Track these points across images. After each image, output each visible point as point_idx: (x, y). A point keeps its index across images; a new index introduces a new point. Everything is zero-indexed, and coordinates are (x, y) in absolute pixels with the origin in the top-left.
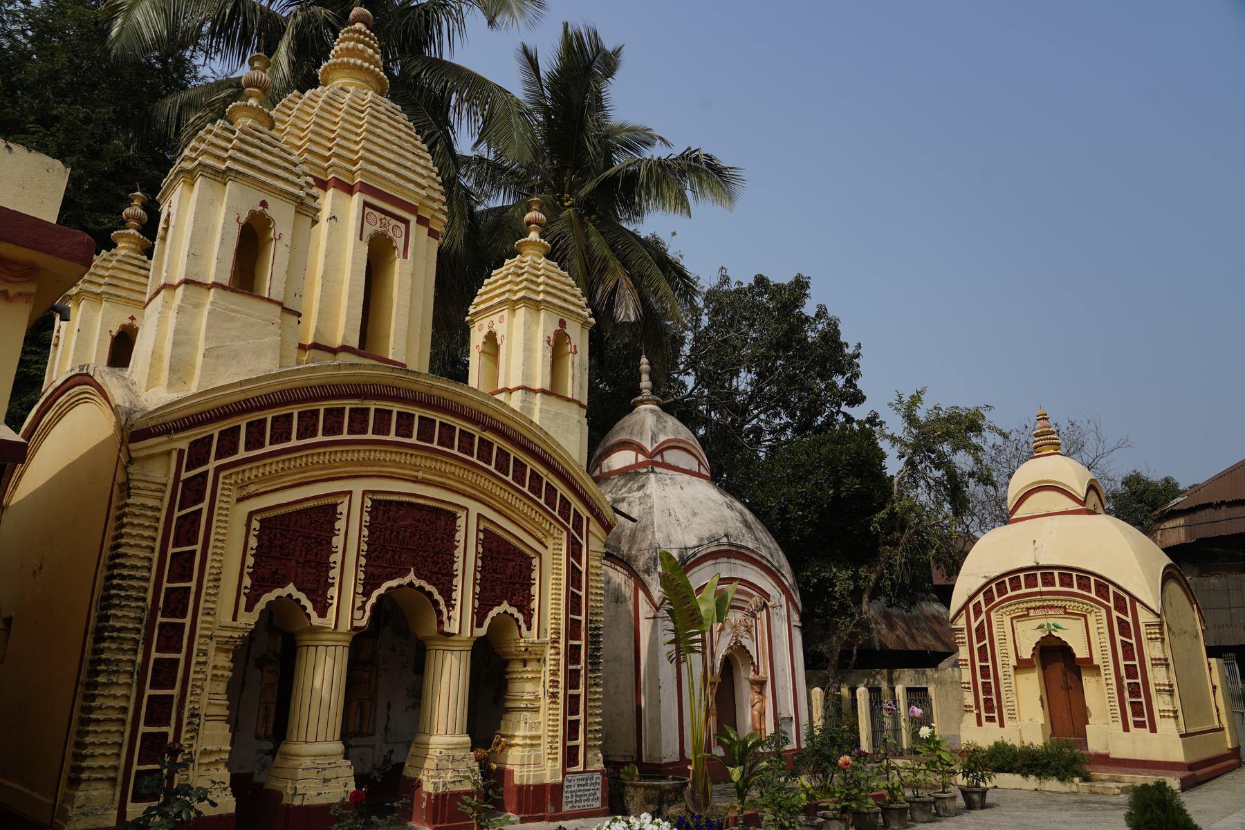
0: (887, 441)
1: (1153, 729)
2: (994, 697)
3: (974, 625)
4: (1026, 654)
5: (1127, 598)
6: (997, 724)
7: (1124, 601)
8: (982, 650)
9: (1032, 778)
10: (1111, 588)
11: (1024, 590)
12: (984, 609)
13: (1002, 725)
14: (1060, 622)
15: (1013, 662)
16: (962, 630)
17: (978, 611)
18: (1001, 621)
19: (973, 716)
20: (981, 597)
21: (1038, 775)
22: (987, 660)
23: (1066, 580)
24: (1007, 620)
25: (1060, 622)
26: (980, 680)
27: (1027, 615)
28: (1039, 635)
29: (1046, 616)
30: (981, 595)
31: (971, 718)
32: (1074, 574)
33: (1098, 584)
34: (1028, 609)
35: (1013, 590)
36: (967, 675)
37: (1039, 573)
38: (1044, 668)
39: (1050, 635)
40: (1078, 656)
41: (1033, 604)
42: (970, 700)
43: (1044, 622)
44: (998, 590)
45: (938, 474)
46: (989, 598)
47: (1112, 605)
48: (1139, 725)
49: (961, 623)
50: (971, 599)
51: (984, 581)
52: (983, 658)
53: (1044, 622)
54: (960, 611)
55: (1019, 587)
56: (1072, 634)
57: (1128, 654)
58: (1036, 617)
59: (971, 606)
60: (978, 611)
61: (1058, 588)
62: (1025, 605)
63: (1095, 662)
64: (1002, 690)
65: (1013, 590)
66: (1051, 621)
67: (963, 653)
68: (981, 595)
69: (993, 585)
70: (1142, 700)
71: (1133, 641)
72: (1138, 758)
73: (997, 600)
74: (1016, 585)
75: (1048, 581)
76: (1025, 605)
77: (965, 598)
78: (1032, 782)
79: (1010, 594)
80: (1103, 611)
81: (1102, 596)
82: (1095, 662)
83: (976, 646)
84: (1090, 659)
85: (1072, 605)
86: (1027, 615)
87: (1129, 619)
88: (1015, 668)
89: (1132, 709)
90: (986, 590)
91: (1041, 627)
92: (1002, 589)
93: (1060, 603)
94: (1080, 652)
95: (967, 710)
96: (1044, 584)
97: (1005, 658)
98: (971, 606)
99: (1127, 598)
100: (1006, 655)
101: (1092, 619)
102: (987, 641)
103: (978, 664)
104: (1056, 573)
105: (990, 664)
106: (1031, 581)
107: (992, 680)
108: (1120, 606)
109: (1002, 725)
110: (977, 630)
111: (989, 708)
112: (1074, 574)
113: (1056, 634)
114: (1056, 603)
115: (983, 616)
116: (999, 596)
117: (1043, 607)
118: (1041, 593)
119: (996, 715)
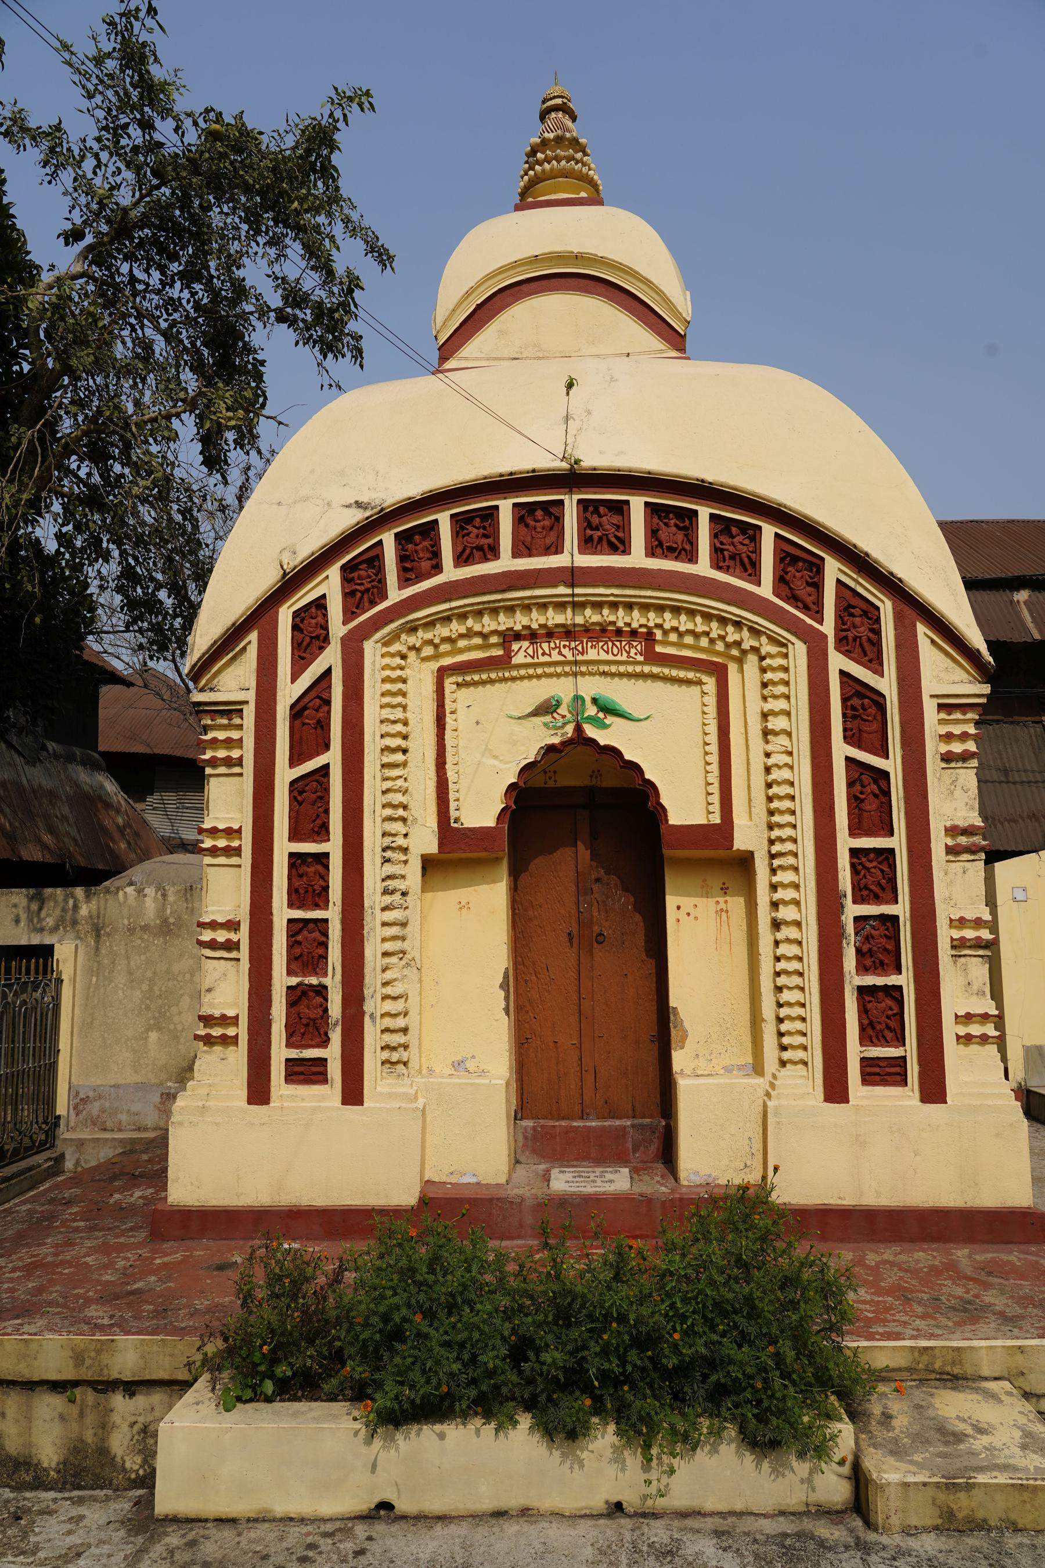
0: (34, 154)
1: (934, 1091)
2: (333, 982)
3: (289, 691)
4: (481, 808)
5: (887, 608)
6: (331, 1092)
7: (871, 607)
8: (309, 792)
9: (605, 1438)
10: (833, 569)
11: (506, 562)
12: (337, 627)
13: (353, 1095)
14: (621, 692)
15: (425, 839)
16: (231, 711)
17: (310, 635)
18: (397, 681)
19: (238, 1058)
20: (330, 584)
21: (639, 1432)
22: (322, 832)
23: (670, 534)
24: (421, 679)
25: (621, 692)
26: (282, 913)
27: (503, 662)
28: (533, 740)
29: (576, 669)
30: (334, 573)
31: (224, 1071)
32: (704, 512)
33: (786, 556)
34: (510, 637)
35: (462, 559)
36: (226, 892)
37: (571, 503)
38: (516, 874)
39: (580, 739)
40: (676, 817)
41: (536, 619)
42: (227, 989)
43: (562, 689)
44: (403, 558)
45: (178, 285)
46: (363, 584)
47: (828, 627)
48: (883, 1073)
49: (235, 682)
50: (292, 582)
51: (353, 518)
52: (309, 820)
53: (562, 689)
54: (229, 642)
55: (492, 552)
56: (663, 737)
57: (872, 813)
58: (535, 672)
59: (285, 616)
60: (310, 635)
61: (637, 557)
62: (504, 622)
63: (742, 841)
64: (372, 950)
65: (462, 559)
66: (590, 687)
67: (227, 802)
68: (334, 573)
69: (388, 539)
70: (905, 979)
71: (893, 765)
72: (872, 1198)
73: (395, 594)
74: (477, 538)
75: (604, 530)
76: (504, 622)
77: (268, 580)
78: (603, 1467)
79: (451, 573)
80: (799, 651)
81: (793, 598)
82: (742, 841)
83: (284, 775)
84: (725, 829)
85: (680, 632)
86: (503, 662)
87: (887, 684)
88: (428, 864)
89: (863, 1010)
90: (353, 555)
91: (547, 708)
92: (418, 553)
93: (637, 619)
94: (685, 804)
95: (214, 1031)
96: (588, 544)
97: (400, 821)
98: (285, 616)
99: (887, 608)
100: (399, 813)
101: (744, 683)
102: (333, 757)
103: (283, 847)
104: (637, 503)
105: (334, 847)
106: (538, 528)
107: (333, 914)
108: (859, 635)
109: (353, 1095)
110: (297, 710)
111: (307, 1025)
112: (704, 512)
113: (603, 738)
114: (621, 618)
115: (331, 657)
116: (405, 581)
117: (568, 633)
118: (572, 576)
119: (333, 1053)
